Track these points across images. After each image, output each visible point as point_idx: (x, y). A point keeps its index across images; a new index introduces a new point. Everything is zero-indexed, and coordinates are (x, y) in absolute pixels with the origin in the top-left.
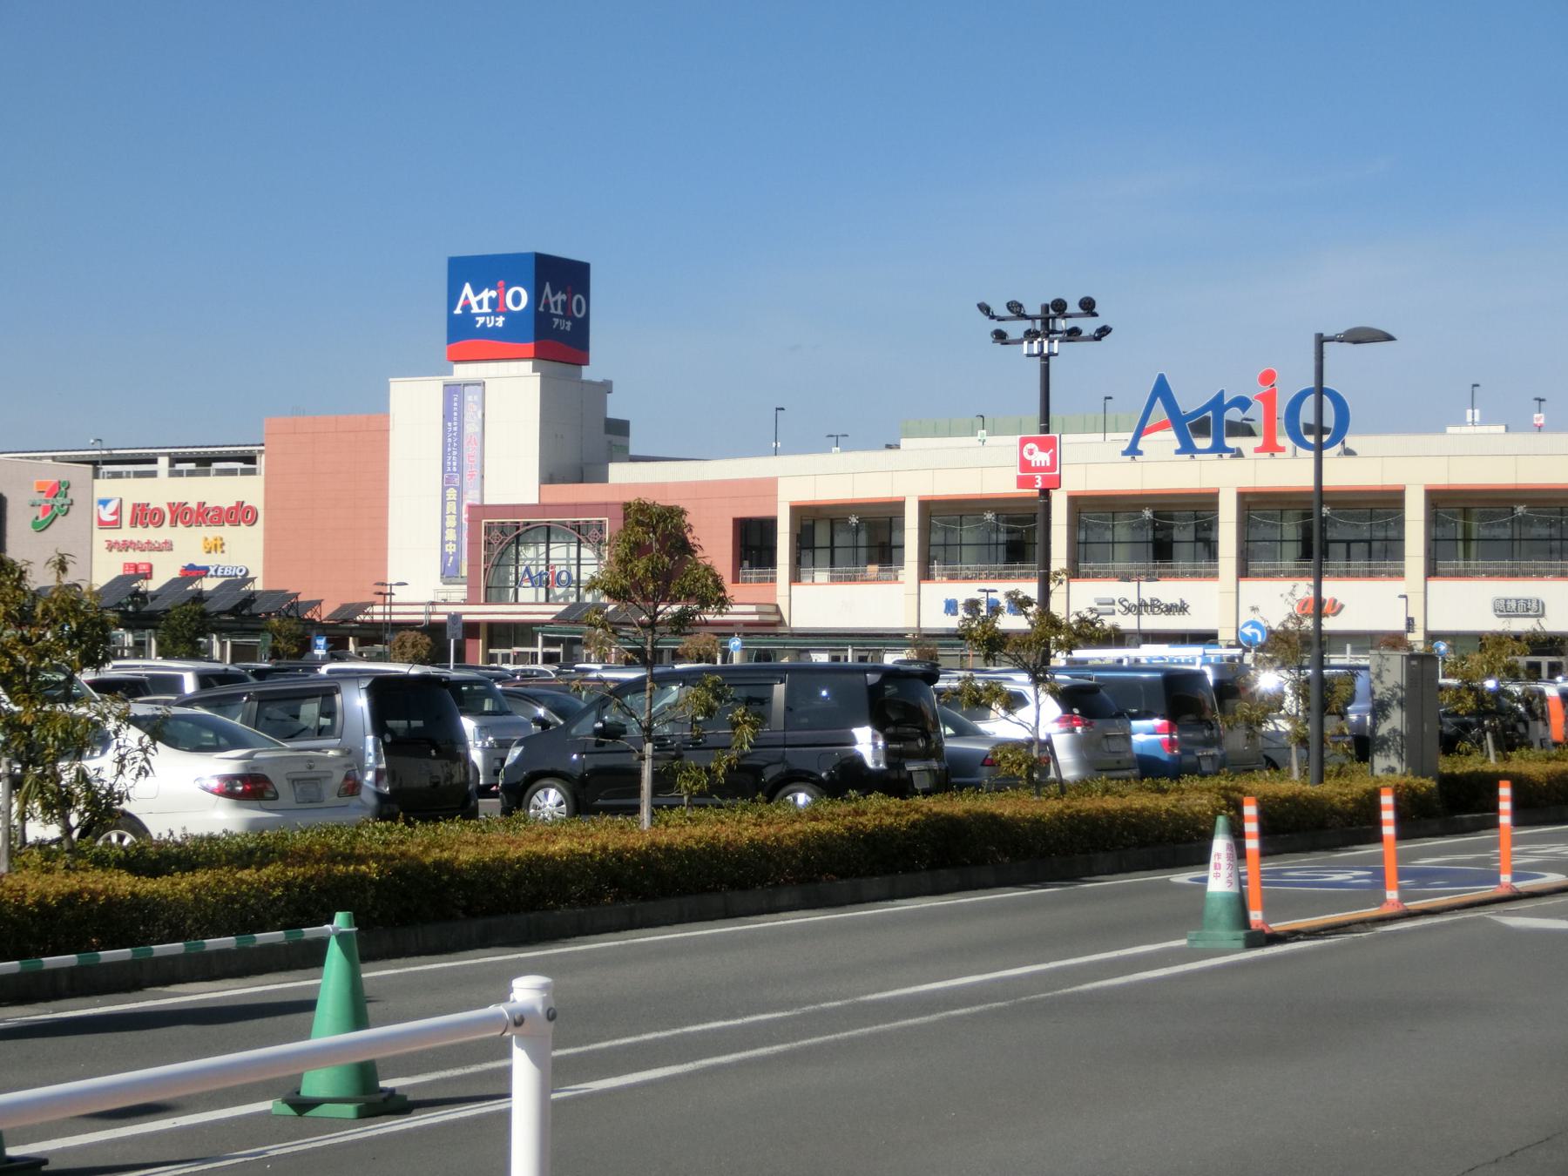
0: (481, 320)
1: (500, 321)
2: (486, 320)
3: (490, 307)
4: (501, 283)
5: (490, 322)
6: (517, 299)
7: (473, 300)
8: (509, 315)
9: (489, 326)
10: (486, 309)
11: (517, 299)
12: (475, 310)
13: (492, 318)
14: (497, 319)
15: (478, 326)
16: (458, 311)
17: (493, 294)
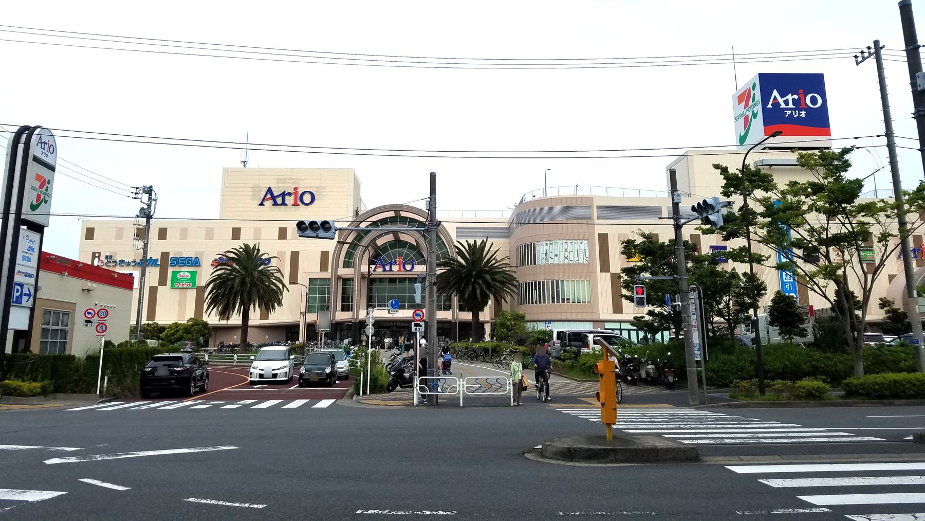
0: (789, 112)
1: (803, 113)
2: (792, 113)
3: (793, 105)
4: (801, 91)
5: (796, 114)
6: (814, 101)
7: (781, 100)
8: (808, 109)
9: (795, 116)
10: (791, 106)
11: (814, 101)
12: (783, 106)
13: (797, 111)
14: (800, 112)
15: (786, 116)
16: (769, 106)
17: (796, 97)
